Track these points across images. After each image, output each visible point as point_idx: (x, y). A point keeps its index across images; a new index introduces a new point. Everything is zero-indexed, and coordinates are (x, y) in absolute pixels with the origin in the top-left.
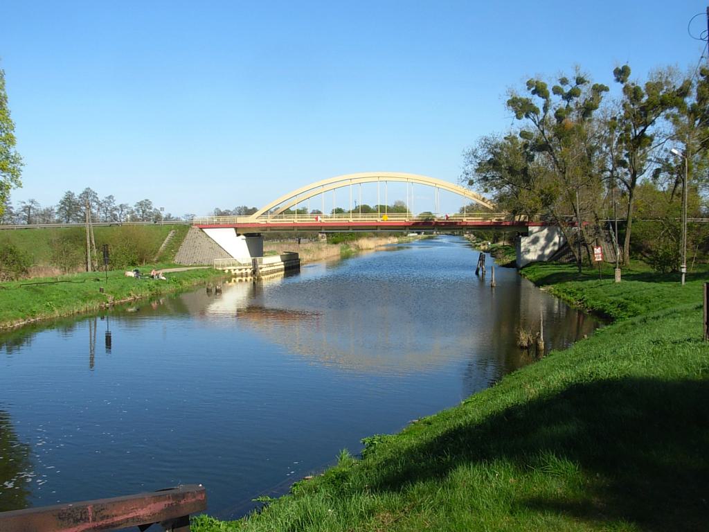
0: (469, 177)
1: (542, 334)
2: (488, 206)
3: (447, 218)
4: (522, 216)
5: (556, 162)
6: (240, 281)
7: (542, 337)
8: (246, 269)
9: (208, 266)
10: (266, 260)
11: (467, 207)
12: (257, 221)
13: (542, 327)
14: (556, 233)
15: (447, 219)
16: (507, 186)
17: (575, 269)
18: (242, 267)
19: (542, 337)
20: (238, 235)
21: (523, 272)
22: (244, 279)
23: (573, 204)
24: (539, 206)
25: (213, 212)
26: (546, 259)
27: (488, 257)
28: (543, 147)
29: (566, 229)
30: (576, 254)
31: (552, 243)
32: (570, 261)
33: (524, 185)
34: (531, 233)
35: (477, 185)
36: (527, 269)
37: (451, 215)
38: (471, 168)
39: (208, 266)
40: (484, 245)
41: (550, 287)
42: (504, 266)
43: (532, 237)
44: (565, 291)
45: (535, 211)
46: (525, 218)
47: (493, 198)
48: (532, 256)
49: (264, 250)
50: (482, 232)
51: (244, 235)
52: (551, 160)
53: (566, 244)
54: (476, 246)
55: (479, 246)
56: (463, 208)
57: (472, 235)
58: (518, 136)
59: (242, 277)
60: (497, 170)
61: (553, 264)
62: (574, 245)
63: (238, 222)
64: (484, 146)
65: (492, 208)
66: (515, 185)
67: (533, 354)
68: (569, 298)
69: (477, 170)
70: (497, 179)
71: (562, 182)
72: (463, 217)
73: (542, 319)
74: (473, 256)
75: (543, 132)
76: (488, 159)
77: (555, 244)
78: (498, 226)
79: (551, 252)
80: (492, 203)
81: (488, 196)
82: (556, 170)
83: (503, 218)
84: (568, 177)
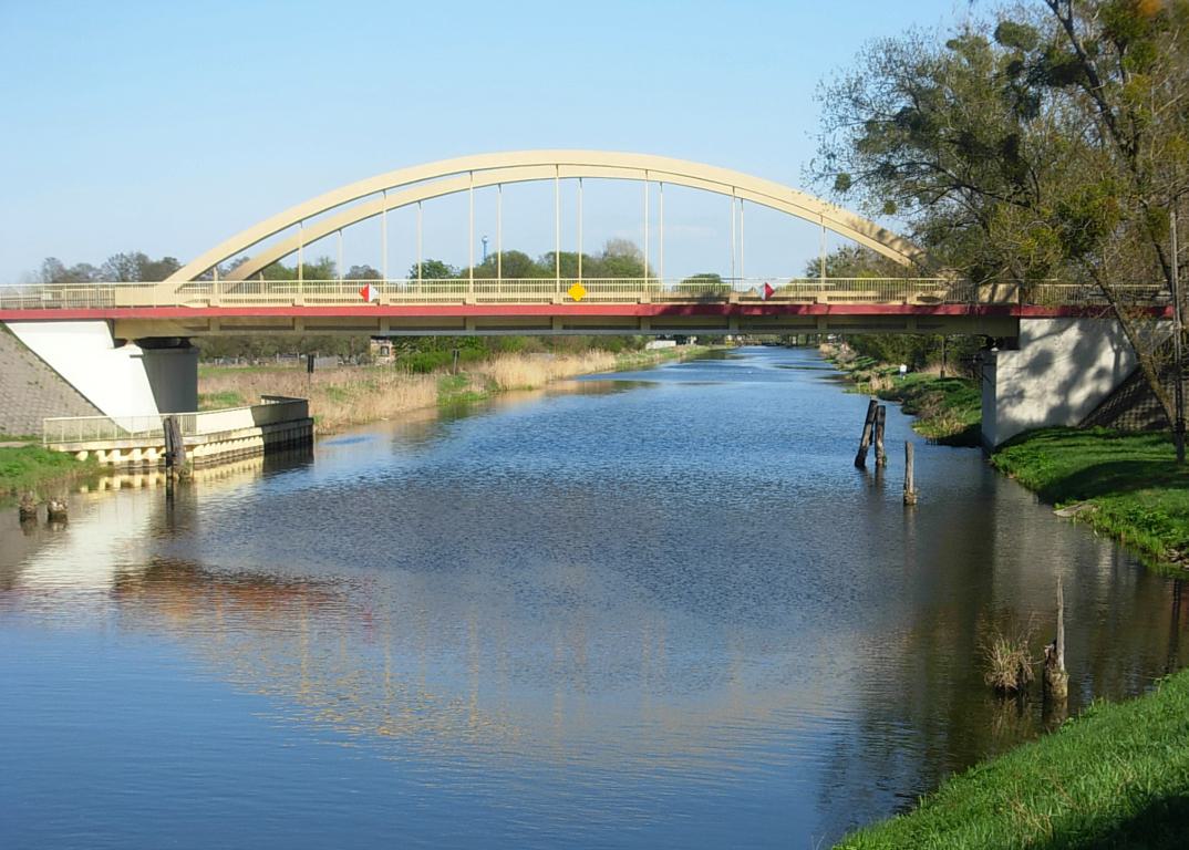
0: (835, 164)
1: (1061, 650)
2: (896, 257)
3: (769, 292)
4: (1001, 287)
5: (1108, 117)
6: (126, 486)
7: (1061, 659)
8: (144, 450)
9: (25, 438)
10: (207, 422)
11: (830, 260)
12: (179, 300)
13: (1061, 629)
14: (1106, 339)
15: (767, 299)
16: (956, 194)
17: (1166, 452)
18: (132, 444)
19: (1061, 659)
20: (119, 343)
21: (1001, 460)
22: (137, 480)
23: (1158, 247)
24: (1053, 256)
25: (40, 270)
26: (1073, 421)
27: (895, 418)
28: (1067, 71)
29: (1138, 327)
30: (1167, 406)
31: (1092, 371)
32: (1148, 427)
33: (1007, 190)
34: (1029, 339)
35: (860, 191)
36: (1014, 450)
37: (780, 282)
38: (842, 138)
39: (25, 438)
40: (882, 376)
41: (1088, 507)
42: (943, 441)
43: (1029, 353)
44: (1132, 519)
45: (1041, 272)
46: (1010, 293)
47: (910, 233)
48: (1030, 411)
49: (201, 390)
50: (877, 336)
51: (139, 342)
52: (1092, 111)
53: (1136, 373)
54: (857, 379)
55: (868, 380)
56: (818, 265)
57: (845, 348)
58: (990, 38)
59: (132, 474)
60: (924, 144)
61: (1096, 435)
62: (1163, 376)
63: (118, 304)
64: (887, 68)
65: (906, 262)
66: (977, 190)
67: (1032, 712)
68: (1145, 539)
69: (861, 146)
70: (922, 172)
71: (1126, 182)
72: (819, 289)
73: (1061, 604)
74: (853, 406)
75: (1068, 24)
76: (897, 110)
77: (1101, 374)
78: (924, 317)
79: (1090, 397)
80: (907, 246)
81: (896, 225)
82: (1107, 142)
83: (940, 294)
84: (1148, 165)
